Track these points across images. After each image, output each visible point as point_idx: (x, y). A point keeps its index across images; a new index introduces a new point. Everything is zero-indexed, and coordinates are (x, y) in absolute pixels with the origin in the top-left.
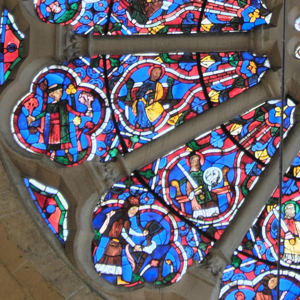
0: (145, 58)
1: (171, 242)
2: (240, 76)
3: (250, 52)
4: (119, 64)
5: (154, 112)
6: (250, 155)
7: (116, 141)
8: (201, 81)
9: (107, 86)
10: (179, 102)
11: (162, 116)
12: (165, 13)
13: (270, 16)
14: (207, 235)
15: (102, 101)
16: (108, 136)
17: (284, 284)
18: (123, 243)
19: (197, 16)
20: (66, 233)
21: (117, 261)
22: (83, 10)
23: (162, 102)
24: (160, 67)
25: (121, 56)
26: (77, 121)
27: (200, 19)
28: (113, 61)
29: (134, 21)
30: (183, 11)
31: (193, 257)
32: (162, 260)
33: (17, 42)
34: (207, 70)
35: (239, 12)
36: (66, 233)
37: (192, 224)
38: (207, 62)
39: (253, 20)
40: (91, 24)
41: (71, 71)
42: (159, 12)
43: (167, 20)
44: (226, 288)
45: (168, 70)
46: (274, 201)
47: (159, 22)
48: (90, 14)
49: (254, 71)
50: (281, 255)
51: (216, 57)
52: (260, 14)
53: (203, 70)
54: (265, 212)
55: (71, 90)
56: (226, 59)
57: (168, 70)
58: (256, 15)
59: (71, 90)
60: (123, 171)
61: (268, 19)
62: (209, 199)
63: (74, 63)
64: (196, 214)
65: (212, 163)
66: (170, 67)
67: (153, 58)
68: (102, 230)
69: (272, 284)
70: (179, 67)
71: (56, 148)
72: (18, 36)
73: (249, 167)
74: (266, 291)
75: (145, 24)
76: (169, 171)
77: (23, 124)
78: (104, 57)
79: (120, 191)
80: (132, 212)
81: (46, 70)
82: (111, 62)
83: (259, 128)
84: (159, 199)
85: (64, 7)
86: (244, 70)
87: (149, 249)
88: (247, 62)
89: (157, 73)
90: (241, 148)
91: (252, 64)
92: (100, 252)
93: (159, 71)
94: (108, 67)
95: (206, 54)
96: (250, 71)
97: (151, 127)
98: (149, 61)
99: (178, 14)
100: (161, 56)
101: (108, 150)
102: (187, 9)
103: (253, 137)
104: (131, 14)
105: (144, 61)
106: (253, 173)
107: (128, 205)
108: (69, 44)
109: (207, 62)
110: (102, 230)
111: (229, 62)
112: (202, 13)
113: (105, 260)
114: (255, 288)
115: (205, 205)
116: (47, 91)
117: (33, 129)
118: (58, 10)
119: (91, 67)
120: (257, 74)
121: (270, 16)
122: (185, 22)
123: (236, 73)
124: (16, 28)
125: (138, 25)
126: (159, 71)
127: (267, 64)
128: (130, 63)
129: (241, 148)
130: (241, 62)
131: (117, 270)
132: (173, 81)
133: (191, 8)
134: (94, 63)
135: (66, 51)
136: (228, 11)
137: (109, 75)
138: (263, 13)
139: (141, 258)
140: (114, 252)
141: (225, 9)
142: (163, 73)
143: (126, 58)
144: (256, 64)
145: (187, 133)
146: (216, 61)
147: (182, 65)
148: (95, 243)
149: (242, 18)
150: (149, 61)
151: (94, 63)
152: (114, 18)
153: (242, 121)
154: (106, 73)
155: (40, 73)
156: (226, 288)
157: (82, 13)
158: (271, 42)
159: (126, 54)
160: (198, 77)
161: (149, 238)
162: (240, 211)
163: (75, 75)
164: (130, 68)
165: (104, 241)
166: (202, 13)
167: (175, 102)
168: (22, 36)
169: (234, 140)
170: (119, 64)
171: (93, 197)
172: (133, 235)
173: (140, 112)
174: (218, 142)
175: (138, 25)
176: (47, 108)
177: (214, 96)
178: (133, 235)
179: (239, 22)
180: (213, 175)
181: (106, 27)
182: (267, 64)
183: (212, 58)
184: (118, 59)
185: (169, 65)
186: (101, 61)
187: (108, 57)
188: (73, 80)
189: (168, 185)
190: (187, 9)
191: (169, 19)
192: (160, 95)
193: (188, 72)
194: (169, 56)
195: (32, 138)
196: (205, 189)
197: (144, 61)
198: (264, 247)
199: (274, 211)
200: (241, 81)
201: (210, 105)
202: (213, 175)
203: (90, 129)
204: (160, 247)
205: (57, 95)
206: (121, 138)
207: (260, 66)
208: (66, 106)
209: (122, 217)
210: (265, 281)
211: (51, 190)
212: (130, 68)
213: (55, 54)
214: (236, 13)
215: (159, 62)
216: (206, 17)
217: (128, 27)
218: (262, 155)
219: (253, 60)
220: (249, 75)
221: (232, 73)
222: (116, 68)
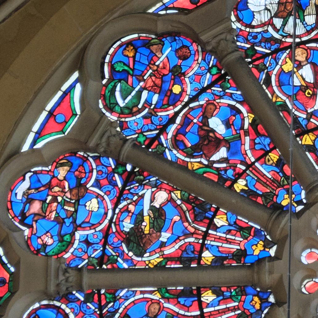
0: (142, 292)
2: (243, 312)
3: (254, 286)
4: (115, 299)
12: (163, 245)
13: (275, 248)
19: (198, 248)
22: (77, 242)
24: (159, 303)
25: (116, 291)
27: (201, 252)
28: (108, 295)
29: (131, 254)
30: (182, 242)
33: (7, 276)
34: (208, 305)
35: (242, 244)
38: (208, 297)
39: (256, 252)
40: (85, 257)
41: (63, 306)
42: (158, 244)
43: (166, 253)
45: (166, 305)
47: (158, 255)
48: (84, 246)
49: (258, 306)
51: (217, 292)
52: (264, 246)
53: (204, 306)
56: (228, 294)
57: (166, 305)
58: (260, 247)
61: (272, 252)
63: (67, 298)
66: (169, 302)
67: (151, 292)
70: (179, 302)
72: (7, 270)
75: (142, 257)
78: (99, 291)
81: (37, 305)
82: (106, 297)
85: (56, 238)
86: (247, 306)
88: (250, 297)
91: (256, 299)
93: (157, 307)
94: (103, 303)
95: (206, 288)
96: (254, 306)
98: (147, 296)
99: (177, 246)
100: (159, 290)
102: (187, 240)
104: (127, 247)
105: (141, 296)
108: (61, 278)
109: (208, 297)
111: (231, 297)
112: (203, 244)
118: (50, 241)
119: (85, 302)
120: (261, 310)
121: (275, 248)
122: (185, 255)
123: (239, 309)
124: (6, 261)
125: (135, 258)
126: (157, 307)
127: (272, 299)
128: (127, 299)
130: (243, 297)
133: (191, 240)
134: (89, 298)
135: (58, 285)
136: (230, 243)
137: (105, 311)
138: (267, 245)
141: (227, 241)
143: (123, 293)
144: (260, 299)
146: (218, 296)
147: (182, 300)
149: (245, 250)
150: (147, 296)
151: (89, 298)
152: (110, 251)
154: (101, 308)
155: (31, 308)
157: (76, 245)
158: (276, 276)
159: (123, 289)
160: (198, 313)
163: (68, 311)
164: (127, 303)
166: (203, 244)
168: (12, 269)
170: (115, 299)
175: (135, 258)
179: (241, 254)
181: (101, 260)
182: (272, 299)
183: (214, 292)
184: (114, 294)
185: (168, 300)
186: (96, 297)
187: (103, 291)
190: (187, 240)
191: (168, 251)
193: (187, 308)
194: (167, 291)
197: (141, 296)
207: (264, 301)
212: (127, 303)
213: (46, 288)
214: (239, 245)
215: (157, 296)
216: (207, 249)
217: (125, 260)
219: (257, 295)
220: (252, 311)
221: (234, 309)
222: (112, 304)
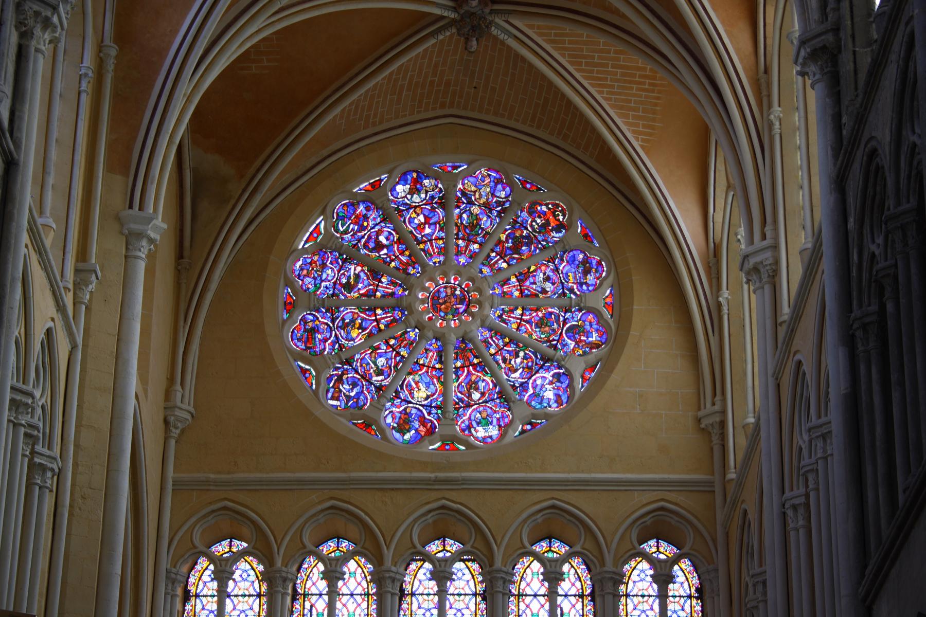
1: (362, 392)
4: (339, 311)
5: (354, 333)
6: (398, 354)
7: (337, 346)
8: (376, 320)
9: (333, 322)
10: (366, 329)
11: (358, 335)
14: (379, 388)
15: (331, 328)
16: (333, 344)
17: (414, 411)
18: (341, 391)
20: (314, 386)
21: (337, 399)
23: (358, 329)
26: (319, 336)
31: (372, 398)
32: (358, 399)
36: (314, 386)
37: (372, 384)
38: (379, 311)
44: (387, 412)
46: (410, 374)
50: (413, 398)
51: (383, 309)
54: (405, 379)
55: (317, 322)
59: (317, 322)
60: (340, 358)
61: (407, 293)
62: (379, 372)
63: (318, 311)
64: (374, 379)
65: (381, 356)
68: (331, 385)
69: (408, 411)
71: (311, 348)
73: (398, 358)
74: (406, 413)
76: (361, 359)
77: (295, 337)
79: (339, 368)
80: (345, 377)
83: (403, 341)
84: (357, 372)
87: (352, 394)
89: (356, 316)
90: (394, 350)
92: (330, 395)
97: (353, 340)
101: (333, 349)
103: (400, 345)
106: (400, 361)
107: (343, 374)
110: (331, 385)
113: (332, 399)
114: (400, 412)
115: (378, 375)
116: (306, 323)
117: (299, 340)
129: (394, 350)
131: (339, 403)
132: (363, 319)
138: (404, 290)
139: (349, 398)
140: (336, 395)
142: (359, 316)
145: (369, 344)
148: (328, 391)
152: (336, 291)
153: (395, 338)
156: (387, 412)
161: (352, 390)
162: (394, 378)
165: (332, 390)
167: (364, 329)
169: (391, 346)
171: (328, 370)
172: (345, 388)
173: (348, 333)
174: (384, 347)
176: (305, 330)
177: (382, 326)
178: (345, 388)
180: (381, 361)
181: (333, 295)
188: (318, 318)
189: (361, 365)
192: (357, 326)
193: (370, 316)
195: (299, 344)
196: (378, 368)
198: (404, 394)
199: (410, 378)
200: (395, 320)
201: (380, 330)
202: (381, 361)
203: (325, 340)
204: (357, 393)
205: (310, 324)
206: (340, 345)
207: (403, 314)
208: (315, 330)
209: (340, 380)
210: (405, 409)
211: (307, 367)
215: (357, 311)
218: (404, 353)
